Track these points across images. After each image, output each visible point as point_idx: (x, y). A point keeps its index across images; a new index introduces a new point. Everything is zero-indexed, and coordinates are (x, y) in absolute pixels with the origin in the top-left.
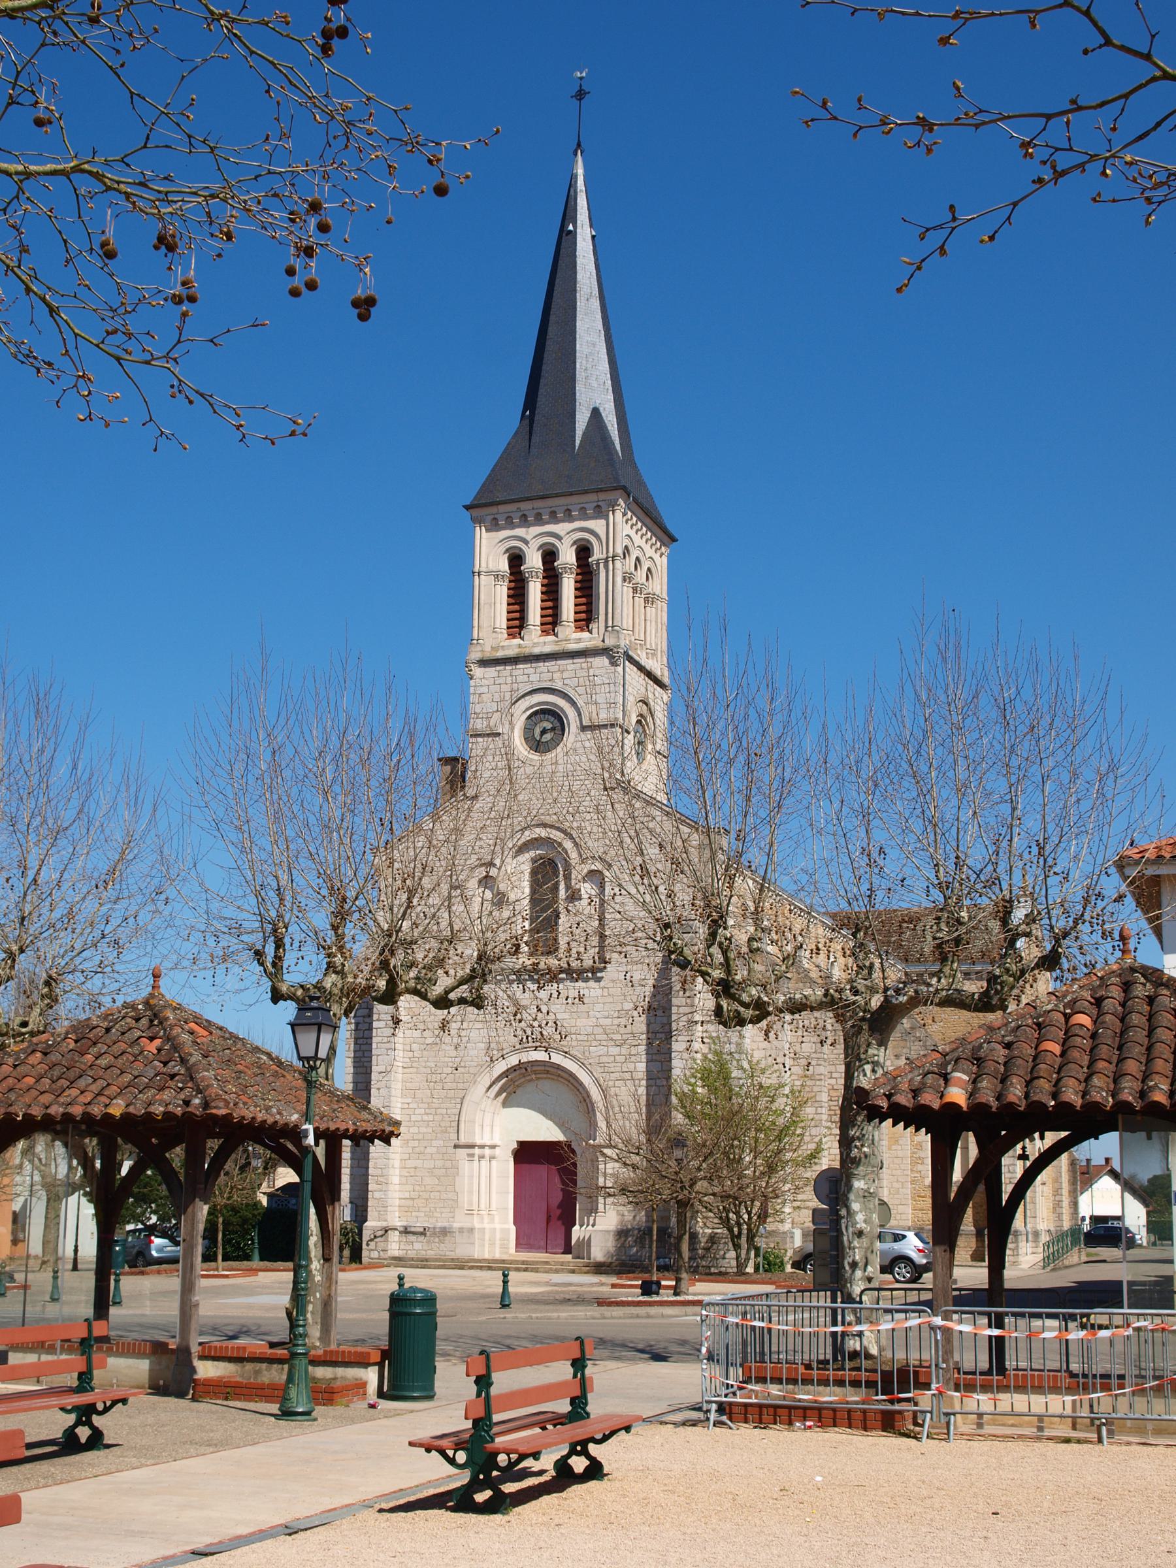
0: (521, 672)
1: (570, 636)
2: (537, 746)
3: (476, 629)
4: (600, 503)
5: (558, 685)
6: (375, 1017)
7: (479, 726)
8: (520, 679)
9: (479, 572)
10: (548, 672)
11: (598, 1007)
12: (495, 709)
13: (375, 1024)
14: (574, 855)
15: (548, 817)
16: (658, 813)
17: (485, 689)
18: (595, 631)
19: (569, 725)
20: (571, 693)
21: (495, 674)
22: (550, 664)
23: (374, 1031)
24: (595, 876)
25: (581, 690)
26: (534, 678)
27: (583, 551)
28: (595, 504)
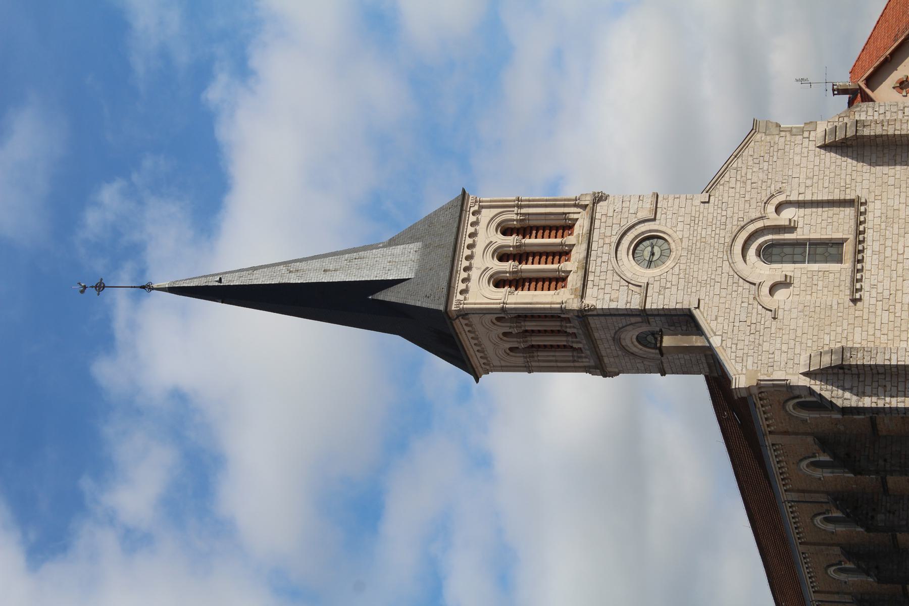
0: (598, 269)
1: (571, 265)
2: (666, 253)
3: (553, 306)
4: (471, 212)
5: (615, 239)
6: (887, 363)
7: (638, 301)
8: (604, 269)
9: (504, 303)
10: (603, 247)
11: (890, 203)
12: (626, 288)
13: (894, 362)
14: (759, 224)
15: (726, 244)
16: (735, 165)
17: (607, 297)
18: (575, 216)
19: (650, 231)
20: (625, 228)
21: (596, 288)
22: (594, 246)
23: (899, 363)
24: (779, 208)
25: (623, 222)
26: (605, 258)
27: (506, 231)
28: (471, 214)
